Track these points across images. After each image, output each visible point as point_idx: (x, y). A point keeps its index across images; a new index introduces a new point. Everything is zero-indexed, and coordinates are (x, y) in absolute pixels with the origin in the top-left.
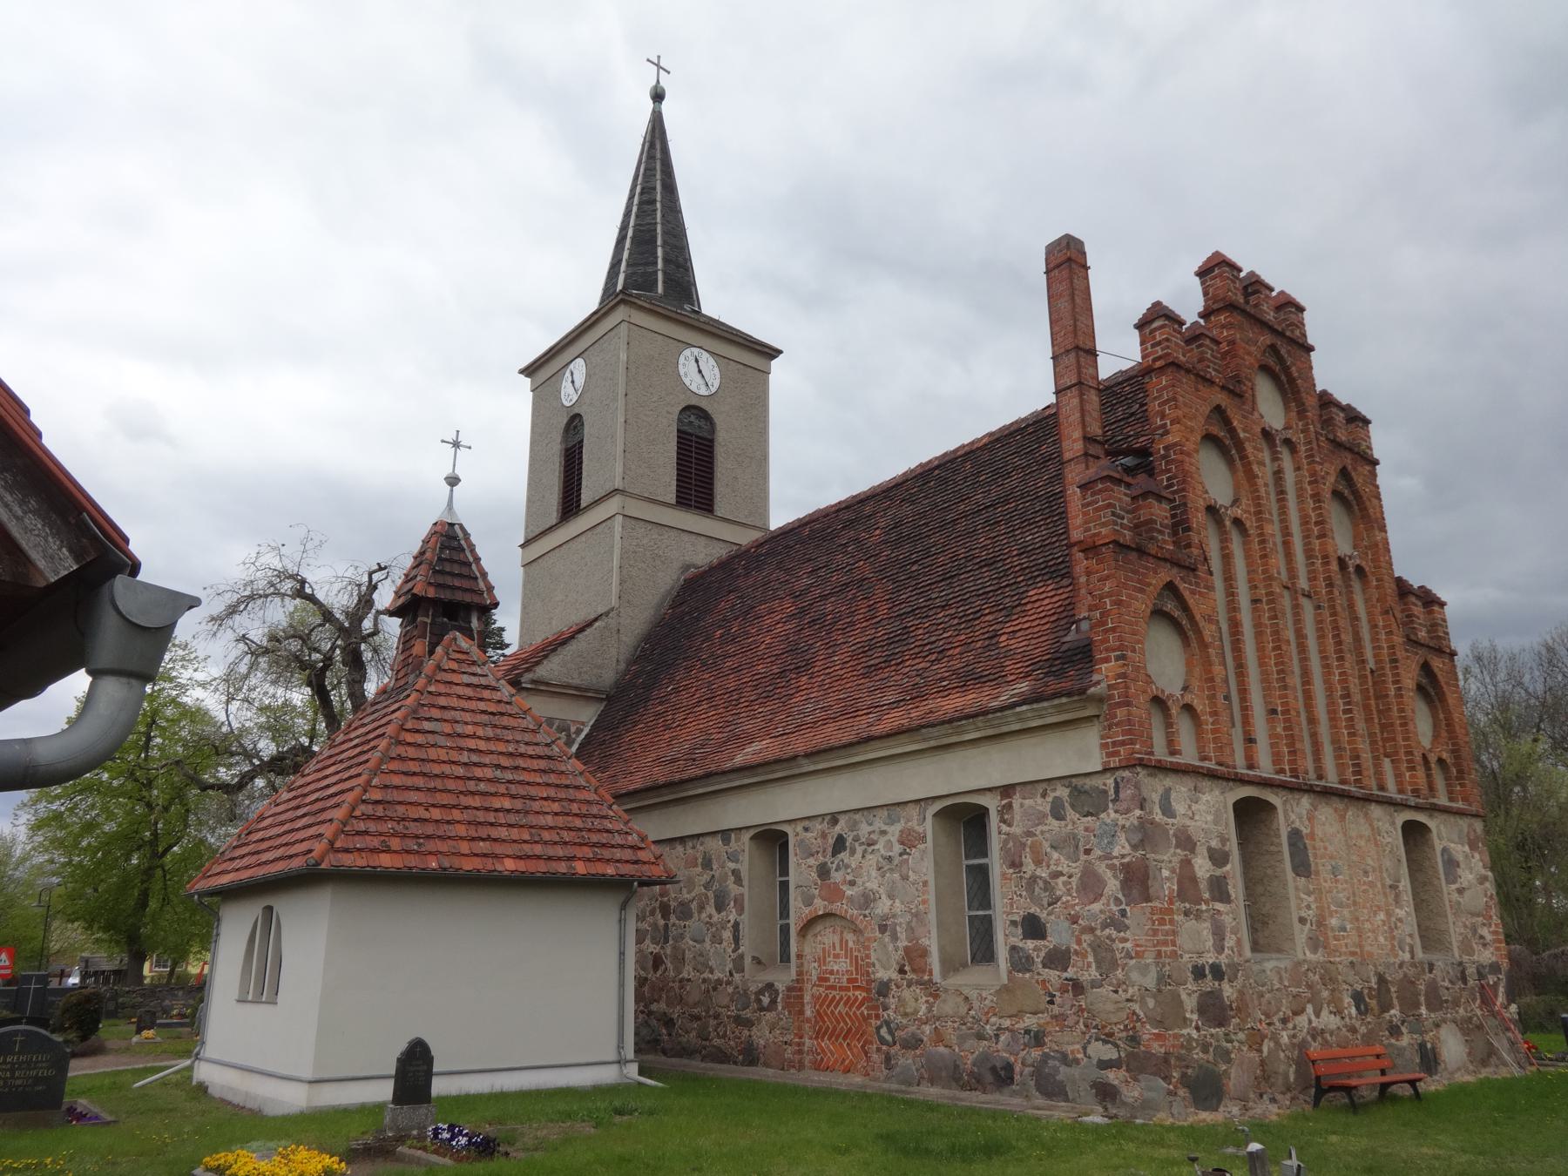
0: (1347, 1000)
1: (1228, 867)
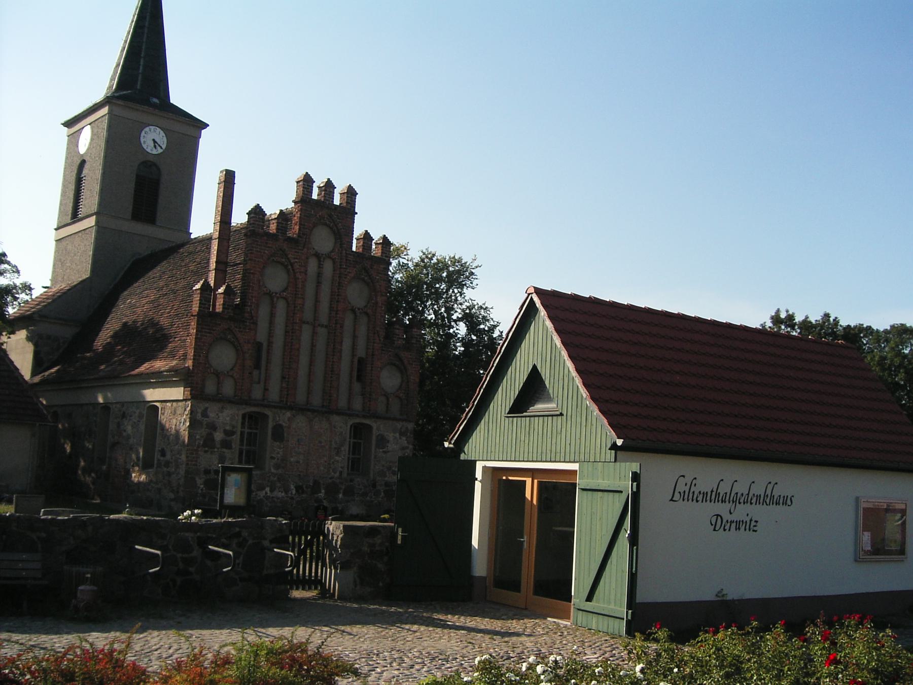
0: (292, 487)
1: (233, 437)
